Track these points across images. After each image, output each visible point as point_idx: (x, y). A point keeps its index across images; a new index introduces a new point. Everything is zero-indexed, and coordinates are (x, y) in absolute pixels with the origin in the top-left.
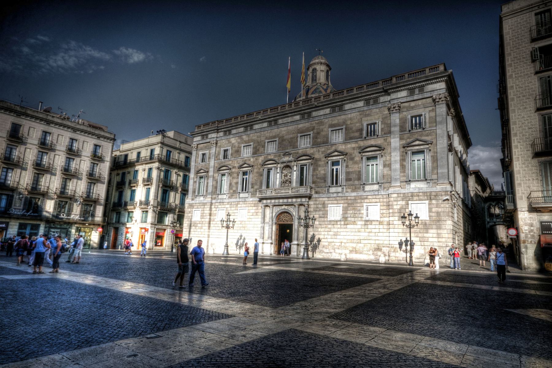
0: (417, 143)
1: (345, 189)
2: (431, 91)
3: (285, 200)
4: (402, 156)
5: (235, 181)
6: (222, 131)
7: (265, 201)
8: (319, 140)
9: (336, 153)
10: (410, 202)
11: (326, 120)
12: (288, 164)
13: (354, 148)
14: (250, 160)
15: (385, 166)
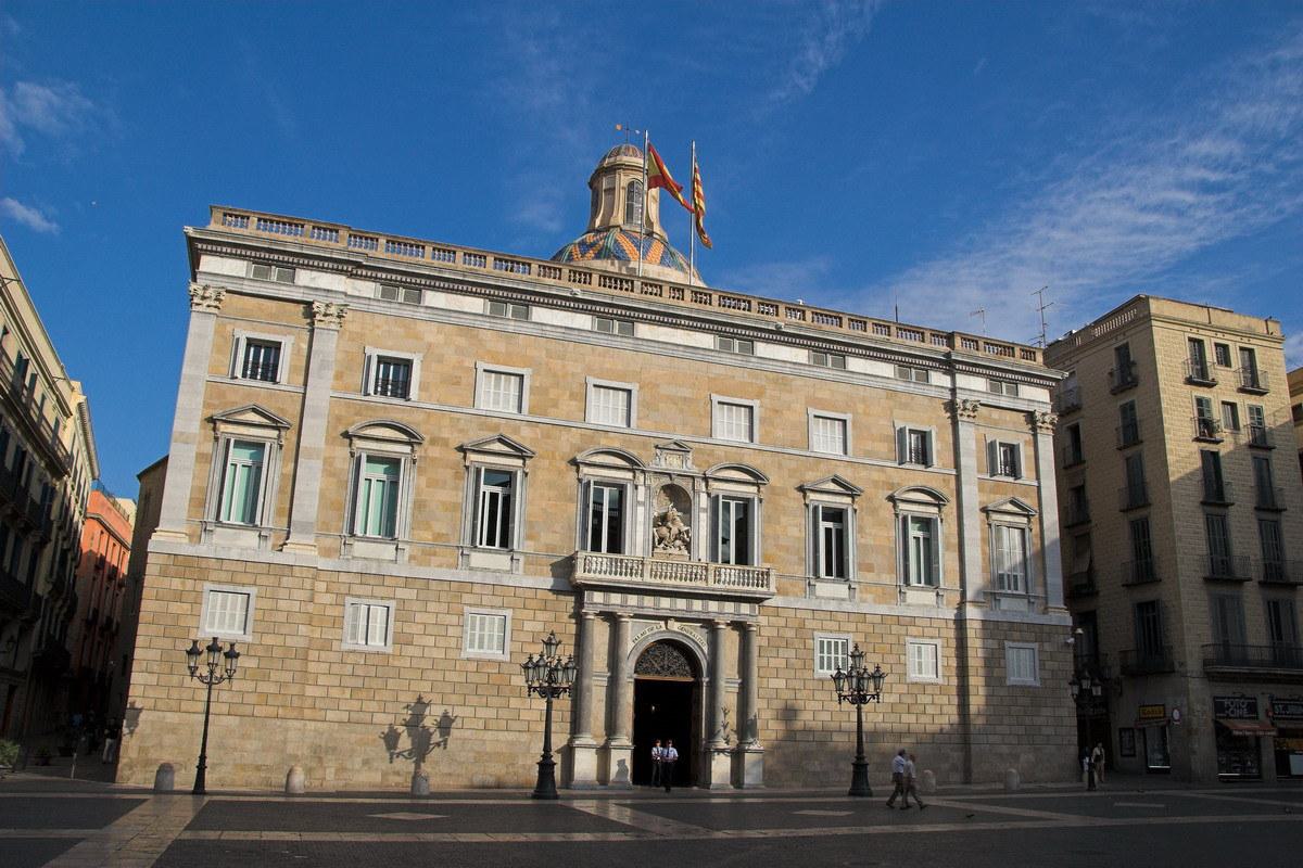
0: (1010, 507)
1: (857, 590)
2: (1029, 400)
3: (681, 603)
4: (982, 530)
5: (445, 495)
6: (375, 279)
7: (598, 597)
8: (780, 434)
9: (832, 487)
10: (1007, 644)
11: (799, 382)
12: (678, 481)
13: (876, 484)
14: (516, 430)
15: (947, 548)
